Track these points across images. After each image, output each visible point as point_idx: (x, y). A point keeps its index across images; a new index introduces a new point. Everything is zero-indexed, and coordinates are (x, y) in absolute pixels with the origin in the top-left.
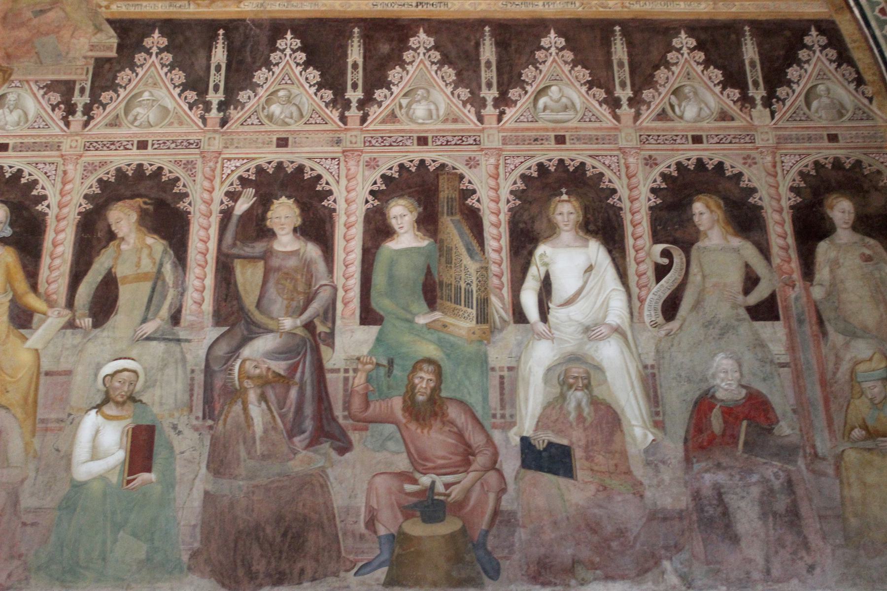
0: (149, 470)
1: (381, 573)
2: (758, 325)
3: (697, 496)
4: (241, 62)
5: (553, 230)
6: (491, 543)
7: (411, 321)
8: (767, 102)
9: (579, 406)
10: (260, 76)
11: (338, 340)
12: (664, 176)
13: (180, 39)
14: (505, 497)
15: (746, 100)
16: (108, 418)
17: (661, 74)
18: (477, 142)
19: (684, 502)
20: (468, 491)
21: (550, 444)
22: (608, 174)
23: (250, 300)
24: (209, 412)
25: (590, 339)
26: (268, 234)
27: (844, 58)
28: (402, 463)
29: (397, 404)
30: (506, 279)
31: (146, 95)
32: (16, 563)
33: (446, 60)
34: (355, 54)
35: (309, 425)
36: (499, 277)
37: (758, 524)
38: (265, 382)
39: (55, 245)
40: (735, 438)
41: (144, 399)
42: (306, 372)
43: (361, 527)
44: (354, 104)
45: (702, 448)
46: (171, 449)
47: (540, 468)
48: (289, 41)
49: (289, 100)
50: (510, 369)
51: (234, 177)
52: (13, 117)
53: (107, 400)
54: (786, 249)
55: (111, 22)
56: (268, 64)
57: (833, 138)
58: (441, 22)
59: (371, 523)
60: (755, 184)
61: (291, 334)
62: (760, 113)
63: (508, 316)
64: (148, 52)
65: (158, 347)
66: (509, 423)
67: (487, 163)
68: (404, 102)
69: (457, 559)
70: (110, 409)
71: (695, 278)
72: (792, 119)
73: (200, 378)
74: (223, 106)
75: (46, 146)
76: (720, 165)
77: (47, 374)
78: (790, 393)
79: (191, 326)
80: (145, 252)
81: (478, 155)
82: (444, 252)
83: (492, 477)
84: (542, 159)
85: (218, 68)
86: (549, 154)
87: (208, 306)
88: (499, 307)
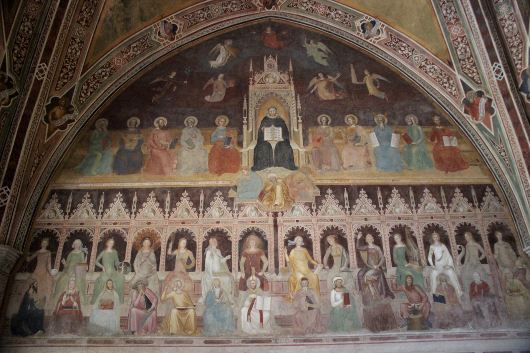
0: (349, 304)
1: (406, 327)
2: (483, 265)
3: (474, 307)
4: (352, 197)
5: (433, 242)
6: (430, 319)
7: (404, 266)
8: (479, 207)
9: (445, 286)
10: (357, 201)
11: (388, 271)
12: (457, 227)
13: (335, 191)
14: (431, 309)
15: (474, 206)
16: (337, 291)
17: (453, 199)
18: (412, 219)
19: (471, 309)
20: (423, 307)
21: (440, 296)
22: (444, 227)
23: (365, 261)
24: (361, 289)
25: (445, 269)
26: (366, 244)
27: (496, 195)
28: (407, 301)
29: (404, 286)
30: (424, 254)
31: (330, 207)
32: (323, 327)
33: (402, 196)
34: (379, 195)
35: (384, 292)
36: (422, 254)
37: (488, 314)
38: (372, 282)
39: (316, 247)
40: (481, 293)
41: (345, 286)
42: (381, 279)
43: (400, 317)
44: (382, 209)
45: (473, 296)
46: (353, 298)
47: (438, 301)
48: (362, 191)
49: (365, 208)
50: (428, 277)
51: (356, 229)
52: (298, 213)
53: (336, 287)
54: (487, 245)
55: (318, 186)
56: (358, 198)
57: (495, 216)
58: (399, 186)
59: (402, 316)
60: (479, 229)
61: (376, 269)
62: (477, 209)
63: (426, 264)
64: (328, 194)
65: (346, 274)
66: (430, 291)
67: (416, 224)
68: (393, 208)
69: (422, 323)
70: (337, 289)
71: (467, 253)
72: (485, 211)
73: (357, 281)
74: (350, 209)
75: (308, 221)
76: (470, 224)
77: (321, 281)
78: (492, 281)
79: (353, 268)
80: (338, 249)
81: (413, 222)
82: (408, 248)
83: (427, 304)
84: (428, 223)
85: (346, 199)
86: (430, 222)
87: (356, 263)
88: (424, 262)
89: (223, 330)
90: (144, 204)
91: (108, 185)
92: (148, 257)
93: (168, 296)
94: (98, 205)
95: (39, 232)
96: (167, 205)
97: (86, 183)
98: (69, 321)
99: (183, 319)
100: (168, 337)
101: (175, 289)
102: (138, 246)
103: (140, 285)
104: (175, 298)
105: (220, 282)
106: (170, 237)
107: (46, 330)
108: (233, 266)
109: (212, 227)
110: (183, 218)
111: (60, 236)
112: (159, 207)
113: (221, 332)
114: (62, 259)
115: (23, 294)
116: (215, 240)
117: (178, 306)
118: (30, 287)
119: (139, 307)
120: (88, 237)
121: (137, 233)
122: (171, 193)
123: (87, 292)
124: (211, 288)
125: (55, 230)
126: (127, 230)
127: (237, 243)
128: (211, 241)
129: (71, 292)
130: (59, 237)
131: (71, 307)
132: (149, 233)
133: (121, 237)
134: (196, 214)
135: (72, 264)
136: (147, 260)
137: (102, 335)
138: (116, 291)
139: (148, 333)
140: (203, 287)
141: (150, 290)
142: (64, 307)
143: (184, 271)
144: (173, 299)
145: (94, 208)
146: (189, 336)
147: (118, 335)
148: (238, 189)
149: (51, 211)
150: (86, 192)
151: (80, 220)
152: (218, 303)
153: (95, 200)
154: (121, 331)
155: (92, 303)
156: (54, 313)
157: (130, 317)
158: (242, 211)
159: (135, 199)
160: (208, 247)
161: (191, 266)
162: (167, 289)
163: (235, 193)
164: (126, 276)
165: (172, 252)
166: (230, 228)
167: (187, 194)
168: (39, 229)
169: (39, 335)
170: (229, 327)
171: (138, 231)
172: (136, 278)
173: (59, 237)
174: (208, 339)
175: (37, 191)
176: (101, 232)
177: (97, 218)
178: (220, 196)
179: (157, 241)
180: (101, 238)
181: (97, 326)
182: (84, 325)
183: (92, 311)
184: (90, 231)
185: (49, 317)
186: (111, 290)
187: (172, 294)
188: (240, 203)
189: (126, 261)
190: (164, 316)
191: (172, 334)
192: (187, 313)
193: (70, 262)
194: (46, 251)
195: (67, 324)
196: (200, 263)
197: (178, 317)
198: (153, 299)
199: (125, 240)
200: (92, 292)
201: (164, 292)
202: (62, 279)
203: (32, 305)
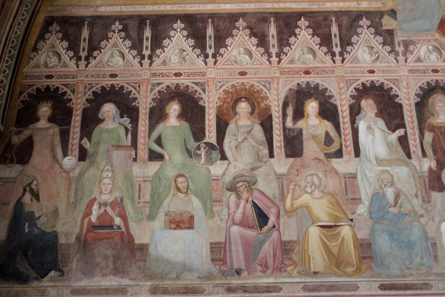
89: (411, 263)
90: (229, 41)
91: (156, 8)
92: (249, 132)
93: (298, 203)
94: (141, 41)
95: (30, 91)
96: (273, 41)
97: (112, 5)
98: (110, 252)
99: (334, 244)
100: (308, 280)
101: (309, 190)
102: (227, 114)
103: (241, 184)
104: (312, 205)
105: (392, 176)
106: (286, 97)
107: (65, 269)
108: (412, 148)
109: (363, 80)
110: (305, 63)
111: (72, 97)
112: (258, 46)
113: (408, 268)
114: (81, 139)
115: (13, 204)
116: (371, 102)
117: (320, 221)
118: (25, 190)
119: (243, 223)
120: (128, 99)
121: (221, 90)
122: (276, 21)
123: (139, 198)
124: (378, 187)
125: (61, 87)
126: (202, 85)
127: (413, 107)
128: (363, 103)
129: (106, 198)
130: (71, 100)
131: (111, 227)
132: (246, 90)
133: (193, 98)
134: (329, 57)
135: (103, 148)
136: (249, 137)
137: (178, 278)
138: (196, 195)
139: (270, 271)
140: (361, 185)
141: (261, 192)
142: (95, 227)
143: (322, 156)
144: (307, 207)
145: (133, 47)
146: (349, 276)
147: (209, 277)
148: (398, 16)
149: (51, 54)
150: (115, 20)
151: (110, 69)
152: (395, 215)
153: (134, 34)
154: (215, 270)
155: (151, 217)
156: (78, 238)
157: (230, 242)
158: (412, 53)
159: (210, 31)
160: (361, 115)
161: (335, 147)
162: (294, 189)
163: (394, 22)
164: (211, 168)
165: (294, 124)
166: (396, 81)
167: (307, 23)
168: (31, 86)
169: (52, 280)
170: (422, 258)
171: (224, 88)
172: (232, 172)
173: (71, 100)
174: (388, 281)
175: (19, 17)
176: (152, 90)
177: (141, 65)
178: (368, 27)
179: (262, 105)
180: (153, 99)
181: (167, 262)
182: (139, 260)
183: (153, 232)
184: (131, 88)
185: (69, 245)
186: (186, 193)
187: (305, 199)
188: (406, 39)
189: (207, 140)
190: (295, 239)
191: (316, 273)
192: (339, 234)
193: (98, 143)
194: (48, 125)
195: (106, 257)
196: (350, 142)
197: (322, 240)
198: (270, 208)
199: (201, 103)
200: (148, 198)
201: (290, 196)
202: (87, 175)
203: (33, 225)
